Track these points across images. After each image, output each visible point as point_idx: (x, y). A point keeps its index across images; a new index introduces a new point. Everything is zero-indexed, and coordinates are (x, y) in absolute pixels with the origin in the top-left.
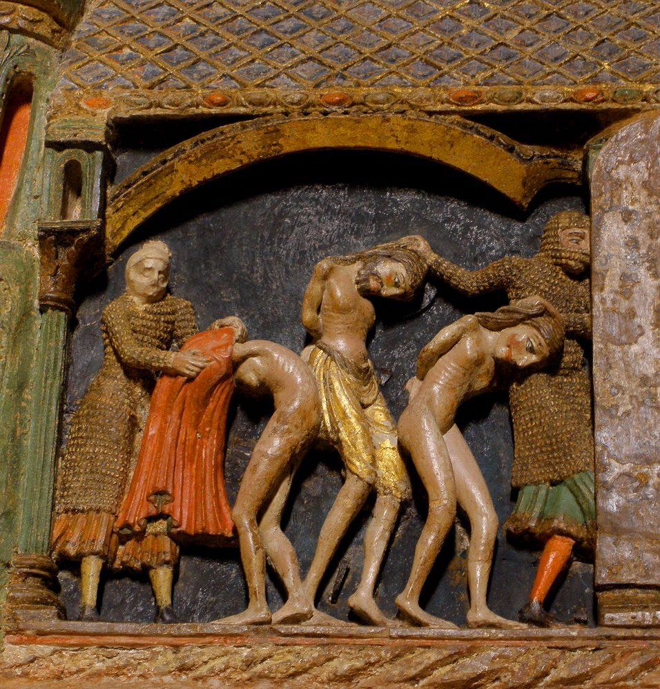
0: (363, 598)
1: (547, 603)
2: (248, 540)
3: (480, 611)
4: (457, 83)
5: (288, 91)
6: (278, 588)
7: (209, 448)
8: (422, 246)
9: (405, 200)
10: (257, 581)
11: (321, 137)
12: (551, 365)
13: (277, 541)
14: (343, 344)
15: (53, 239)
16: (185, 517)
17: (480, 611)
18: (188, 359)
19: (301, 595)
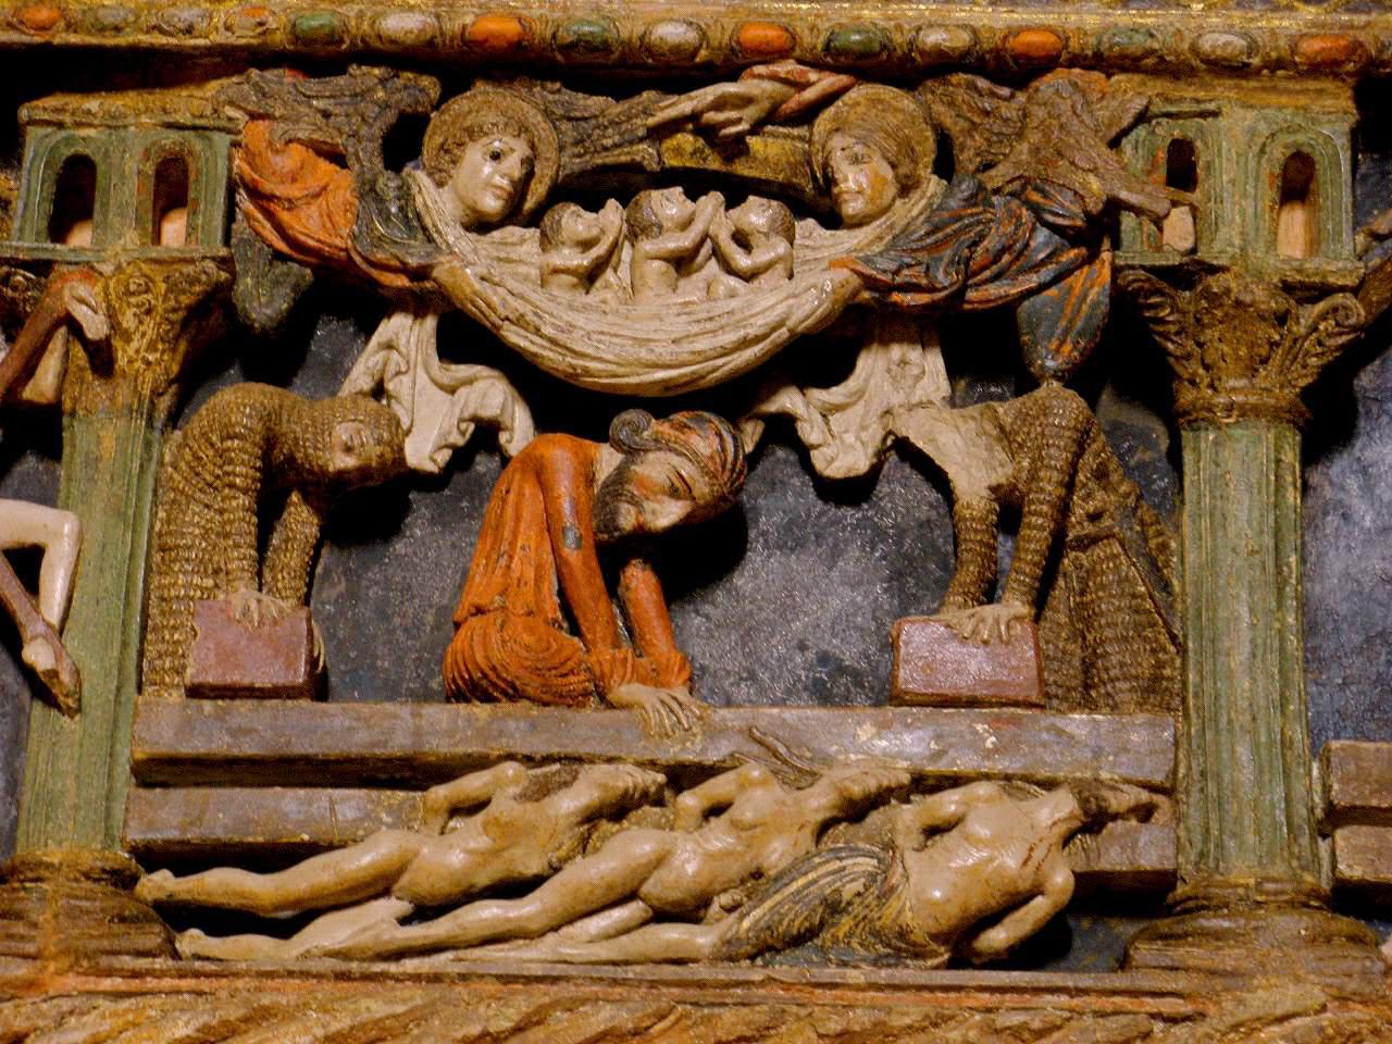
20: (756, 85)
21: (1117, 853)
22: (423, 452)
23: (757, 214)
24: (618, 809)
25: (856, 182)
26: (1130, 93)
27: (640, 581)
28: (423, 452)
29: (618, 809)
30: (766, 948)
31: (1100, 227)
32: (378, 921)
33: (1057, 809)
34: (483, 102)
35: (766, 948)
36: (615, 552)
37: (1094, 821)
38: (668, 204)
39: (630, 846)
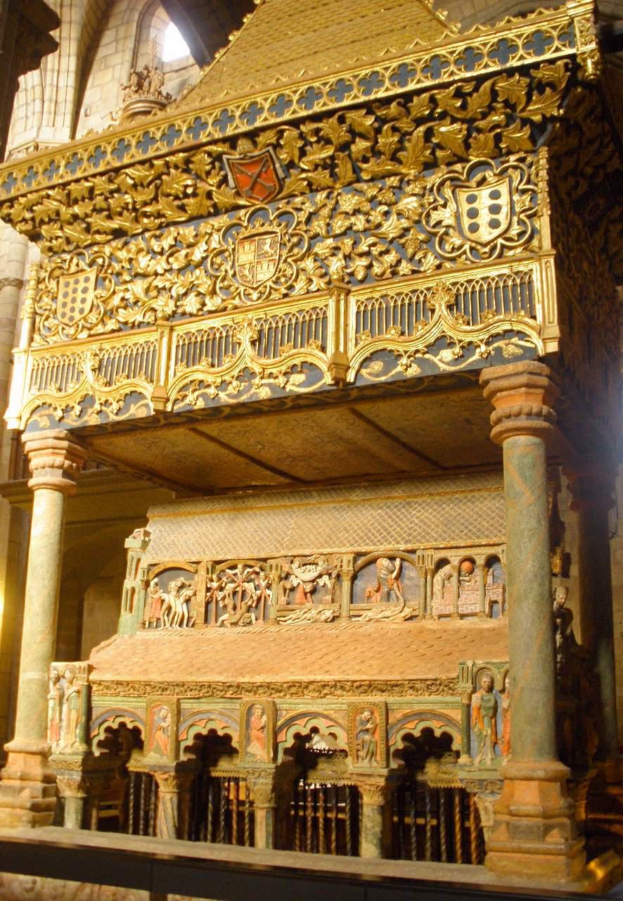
0: (174, 625)
1: (193, 625)
2: (162, 619)
3: (185, 626)
4: (186, 557)
5: (167, 559)
6: (165, 625)
7: (159, 606)
8: (182, 579)
9: (183, 572)
10: (162, 624)
11: (170, 566)
12: (195, 594)
13: (166, 618)
14: (174, 593)
15: (142, 581)
16: (156, 616)
17: (185, 626)
18: (156, 596)
19: (168, 625)
20: (314, 556)
21: (335, 615)
22: (295, 585)
23: (314, 566)
24: (306, 612)
25: (320, 563)
26: (338, 556)
27: (309, 595)
28: (295, 585)
29: (306, 612)
30: (313, 622)
31: (336, 566)
32: (290, 621)
33: (332, 611)
34: (297, 559)
35: (313, 622)
36: (306, 594)
37: (334, 612)
38: (308, 566)
39: (306, 615)
